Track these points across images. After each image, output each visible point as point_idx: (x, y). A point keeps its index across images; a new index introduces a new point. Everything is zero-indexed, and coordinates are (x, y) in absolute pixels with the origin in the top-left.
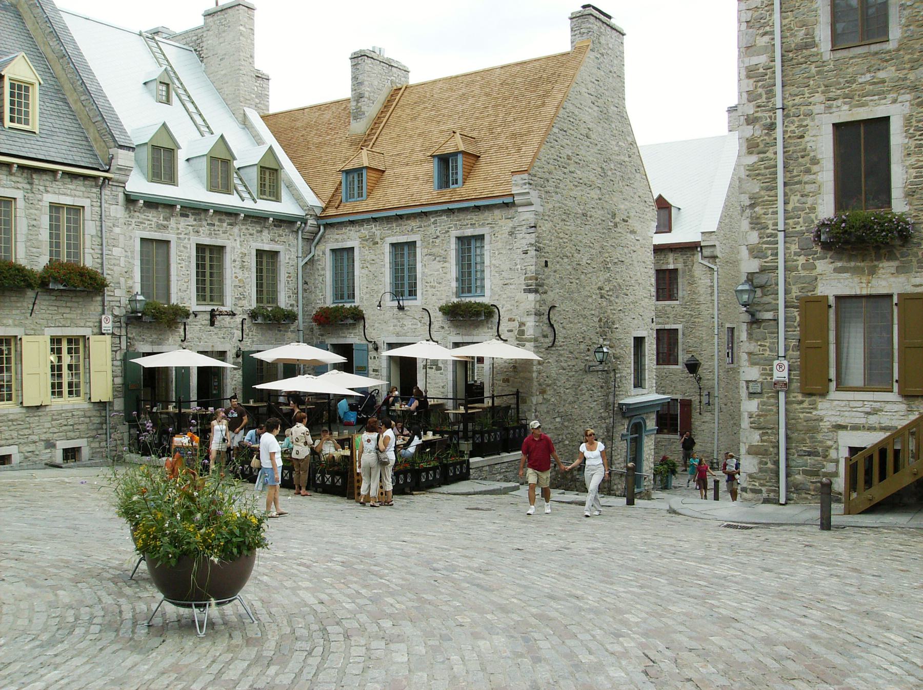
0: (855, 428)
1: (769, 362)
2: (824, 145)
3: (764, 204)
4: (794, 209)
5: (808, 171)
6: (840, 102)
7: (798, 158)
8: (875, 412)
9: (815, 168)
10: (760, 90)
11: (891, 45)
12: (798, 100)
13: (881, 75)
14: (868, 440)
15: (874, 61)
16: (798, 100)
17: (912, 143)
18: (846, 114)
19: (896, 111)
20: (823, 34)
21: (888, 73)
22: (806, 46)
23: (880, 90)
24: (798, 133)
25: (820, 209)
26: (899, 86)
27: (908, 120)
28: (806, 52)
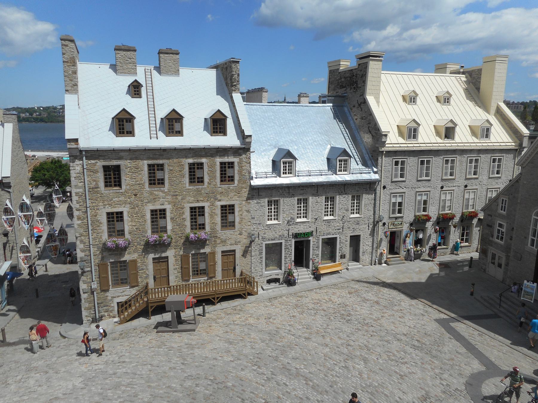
0: (118, 297)
1: (90, 283)
2: (104, 219)
3: (84, 236)
4: (95, 237)
5: (98, 226)
6: (107, 206)
7: (96, 223)
8: (124, 292)
9: (101, 225)
10: (81, 200)
11: (122, 191)
12: (94, 204)
13: (120, 199)
14: (123, 299)
15: (117, 194)
16: (94, 204)
17: (130, 219)
18: (110, 210)
19: (125, 210)
20: (102, 184)
21: (122, 198)
22: (96, 188)
23: (120, 204)
24: (95, 214)
25: (103, 237)
26: (125, 203)
27: (128, 212)
28: (96, 190)
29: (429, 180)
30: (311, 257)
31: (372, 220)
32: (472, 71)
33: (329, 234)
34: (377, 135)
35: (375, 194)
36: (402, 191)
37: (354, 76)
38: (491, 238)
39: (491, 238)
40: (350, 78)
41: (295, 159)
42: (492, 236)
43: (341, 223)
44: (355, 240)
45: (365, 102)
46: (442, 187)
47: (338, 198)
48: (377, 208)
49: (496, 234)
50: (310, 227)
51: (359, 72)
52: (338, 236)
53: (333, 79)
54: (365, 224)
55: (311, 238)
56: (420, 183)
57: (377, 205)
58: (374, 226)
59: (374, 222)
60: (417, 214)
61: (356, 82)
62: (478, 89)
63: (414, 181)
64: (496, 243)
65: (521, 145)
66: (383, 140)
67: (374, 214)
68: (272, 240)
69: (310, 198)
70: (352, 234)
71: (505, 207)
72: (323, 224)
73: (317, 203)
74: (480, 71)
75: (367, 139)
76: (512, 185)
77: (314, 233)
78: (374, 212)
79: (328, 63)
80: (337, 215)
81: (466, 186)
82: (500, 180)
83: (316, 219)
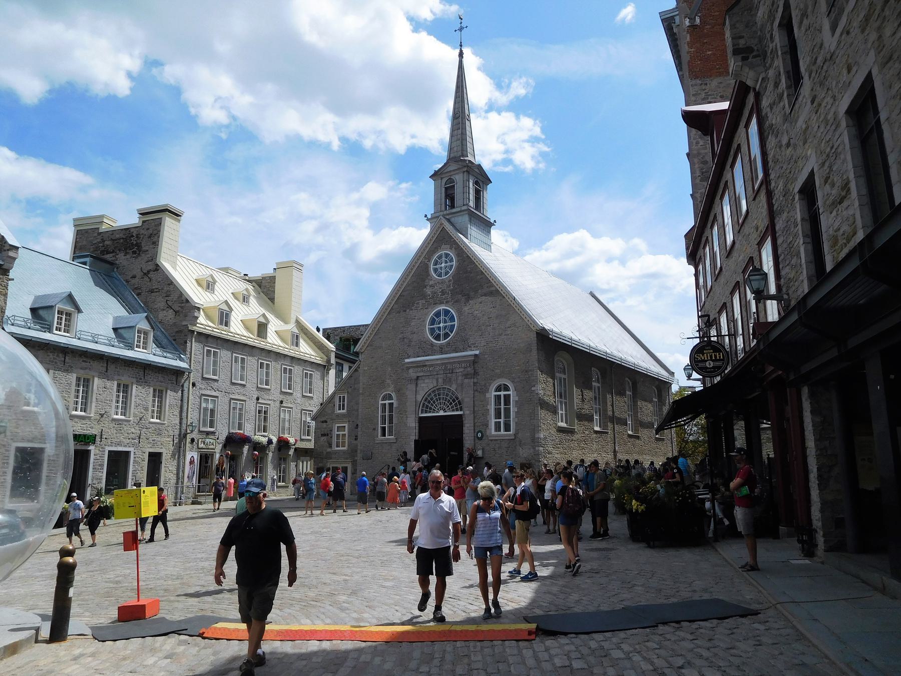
29: (244, 386)
30: (90, 482)
31: (177, 432)
32: (264, 278)
33: (119, 444)
34: (184, 307)
35: (182, 391)
36: (214, 394)
37: (133, 236)
38: (329, 450)
39: (329, 450)
40: (125, 239)
41: (79, 311)
42: (330, 446)
43: (137, 428)
44: (155, 459)
45: (158, 268)
46: (258, 399)
47: (135, 390)
48: (184, 414)
49: (334, 440)
50: (92, 428)
51: (142, 232)
52: (131, 449)
53: (85, 243)
54: (169, 436)
55: (91, 448)
56: (233, 387)
57: (185, 408)
58: (180, 442)
59: (180, 435)
60: (232, 431)
61: (139, 246)
62: (272, 300)
63: (228, 383)
64: (336, 452)
65: (328, 361)
66: (196, 314)
67: (181, 423)
68: (29, 441)
69: (96, 379)
70: (152, 450)
71: (343, 405)
72: (112, 425)
73: (104, 389)
74: (272, 279)
75: (168, 316)
76: (351, 376)
77: (98, 439)
78: (181, 419)
79: (75, 220)
80: (132, 415)
81: (281, 402)
82: (312, 402)
83: (102, 415)
